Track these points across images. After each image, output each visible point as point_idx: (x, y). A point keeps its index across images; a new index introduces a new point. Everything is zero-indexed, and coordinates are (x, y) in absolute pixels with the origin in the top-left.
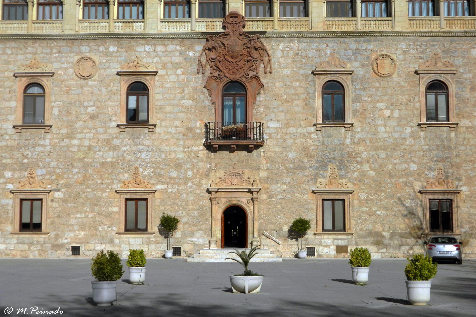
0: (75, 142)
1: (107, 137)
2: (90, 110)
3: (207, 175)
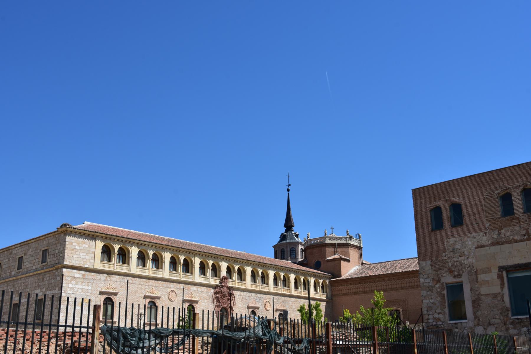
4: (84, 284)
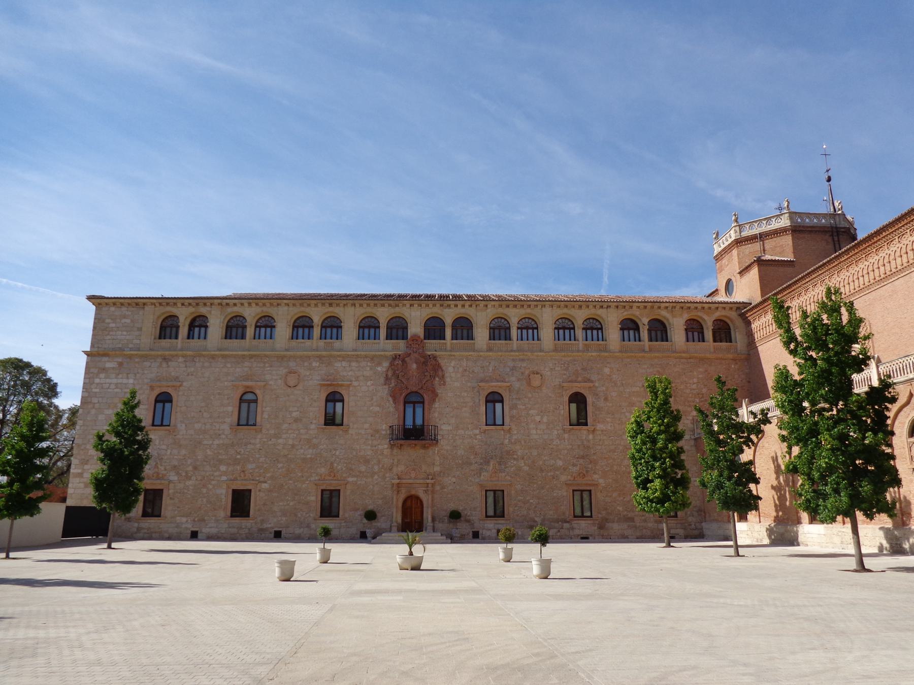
0: (280, 441)
1: (308, 438)
2: (294, 414)
3: (391, 470)
4: (120, 376)
